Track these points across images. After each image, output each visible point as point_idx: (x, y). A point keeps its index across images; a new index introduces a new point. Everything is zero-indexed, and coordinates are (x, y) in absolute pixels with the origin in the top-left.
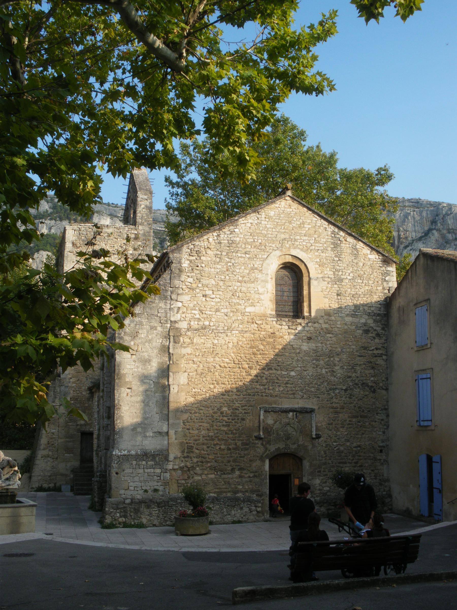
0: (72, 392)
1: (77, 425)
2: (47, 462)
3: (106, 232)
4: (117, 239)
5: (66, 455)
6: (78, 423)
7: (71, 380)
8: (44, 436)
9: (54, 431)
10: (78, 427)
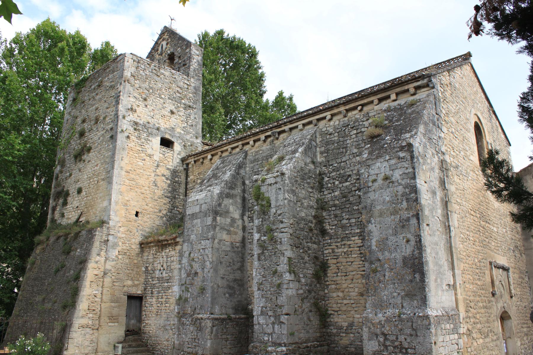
0: (120, 244)
1: (124, 286)
2: (85, 335)
3: (163, 74)
4: (172, 84)
5: (110, 324)
6: (125, 284)
7: (121, 229)
8: (84, 300)
9: (97, 292)
10: (125, 289)
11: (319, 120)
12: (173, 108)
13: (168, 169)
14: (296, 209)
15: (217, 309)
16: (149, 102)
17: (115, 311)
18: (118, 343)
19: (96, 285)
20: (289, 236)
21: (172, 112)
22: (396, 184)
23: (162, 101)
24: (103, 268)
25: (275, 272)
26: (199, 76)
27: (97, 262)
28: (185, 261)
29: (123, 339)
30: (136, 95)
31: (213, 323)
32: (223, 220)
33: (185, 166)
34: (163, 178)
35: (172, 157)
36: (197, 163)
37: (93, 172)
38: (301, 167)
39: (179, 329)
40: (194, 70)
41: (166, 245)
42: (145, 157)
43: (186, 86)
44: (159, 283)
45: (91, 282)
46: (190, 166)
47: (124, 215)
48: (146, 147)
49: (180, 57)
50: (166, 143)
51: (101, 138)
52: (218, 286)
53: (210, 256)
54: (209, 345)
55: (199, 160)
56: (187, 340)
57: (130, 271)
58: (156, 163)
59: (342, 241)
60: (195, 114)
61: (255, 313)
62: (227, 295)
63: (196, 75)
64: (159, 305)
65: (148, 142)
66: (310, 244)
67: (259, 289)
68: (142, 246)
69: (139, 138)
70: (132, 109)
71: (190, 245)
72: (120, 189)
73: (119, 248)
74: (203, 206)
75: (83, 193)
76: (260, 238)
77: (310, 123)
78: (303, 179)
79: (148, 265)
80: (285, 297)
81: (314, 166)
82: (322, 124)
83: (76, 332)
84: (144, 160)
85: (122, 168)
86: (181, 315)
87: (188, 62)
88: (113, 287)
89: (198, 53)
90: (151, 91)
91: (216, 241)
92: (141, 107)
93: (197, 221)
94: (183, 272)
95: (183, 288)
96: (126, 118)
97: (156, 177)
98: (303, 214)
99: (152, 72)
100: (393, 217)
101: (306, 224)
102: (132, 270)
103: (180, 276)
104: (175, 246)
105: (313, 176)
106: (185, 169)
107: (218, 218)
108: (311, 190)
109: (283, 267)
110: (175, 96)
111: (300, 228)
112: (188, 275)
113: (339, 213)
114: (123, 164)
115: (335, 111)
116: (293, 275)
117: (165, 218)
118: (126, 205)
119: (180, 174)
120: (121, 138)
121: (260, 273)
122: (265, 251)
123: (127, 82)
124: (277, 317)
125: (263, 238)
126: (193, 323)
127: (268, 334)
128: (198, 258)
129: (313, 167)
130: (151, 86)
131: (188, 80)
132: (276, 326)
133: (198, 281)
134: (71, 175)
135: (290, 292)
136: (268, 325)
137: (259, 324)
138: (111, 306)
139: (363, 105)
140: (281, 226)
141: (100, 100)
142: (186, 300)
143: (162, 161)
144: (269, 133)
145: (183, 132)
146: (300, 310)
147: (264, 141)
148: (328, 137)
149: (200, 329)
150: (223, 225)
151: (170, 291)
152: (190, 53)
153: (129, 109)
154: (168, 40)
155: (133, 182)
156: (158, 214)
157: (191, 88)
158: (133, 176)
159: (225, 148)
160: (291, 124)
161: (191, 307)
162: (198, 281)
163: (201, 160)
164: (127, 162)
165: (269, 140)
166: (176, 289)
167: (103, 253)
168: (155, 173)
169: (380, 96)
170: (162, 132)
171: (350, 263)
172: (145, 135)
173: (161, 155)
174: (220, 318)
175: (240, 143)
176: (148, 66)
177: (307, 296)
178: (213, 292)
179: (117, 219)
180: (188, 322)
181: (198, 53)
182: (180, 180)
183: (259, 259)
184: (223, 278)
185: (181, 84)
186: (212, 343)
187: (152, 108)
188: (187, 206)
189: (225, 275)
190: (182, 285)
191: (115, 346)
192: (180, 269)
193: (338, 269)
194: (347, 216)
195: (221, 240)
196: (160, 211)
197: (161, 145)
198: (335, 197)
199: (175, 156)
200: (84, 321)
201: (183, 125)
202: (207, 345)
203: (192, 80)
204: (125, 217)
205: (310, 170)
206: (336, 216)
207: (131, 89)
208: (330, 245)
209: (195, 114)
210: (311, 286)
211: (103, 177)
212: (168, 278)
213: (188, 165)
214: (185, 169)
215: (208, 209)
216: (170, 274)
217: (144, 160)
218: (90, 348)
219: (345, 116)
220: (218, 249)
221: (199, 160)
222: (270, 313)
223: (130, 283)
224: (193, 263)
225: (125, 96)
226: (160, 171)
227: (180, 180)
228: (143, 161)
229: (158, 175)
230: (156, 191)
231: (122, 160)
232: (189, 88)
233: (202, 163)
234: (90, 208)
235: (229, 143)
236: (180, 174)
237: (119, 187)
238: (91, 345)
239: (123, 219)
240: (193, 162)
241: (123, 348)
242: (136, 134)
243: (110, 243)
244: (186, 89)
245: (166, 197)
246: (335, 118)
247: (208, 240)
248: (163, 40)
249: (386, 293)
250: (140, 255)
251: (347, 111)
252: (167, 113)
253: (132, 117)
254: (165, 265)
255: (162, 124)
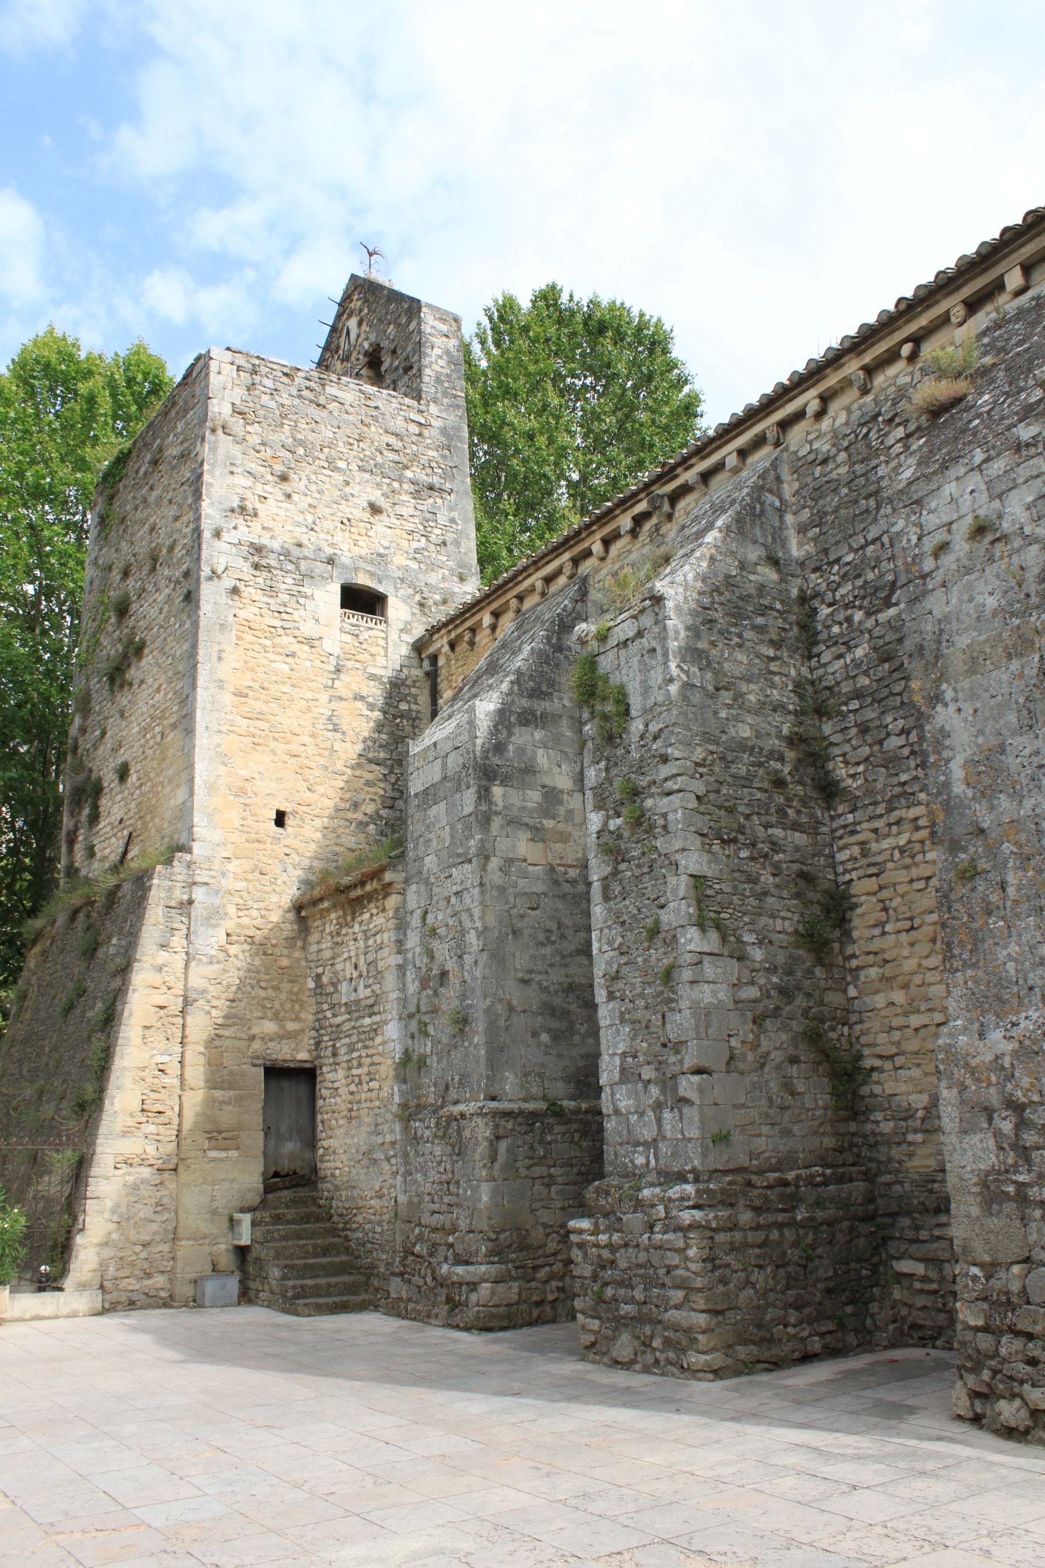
0: (232, 910)
1: (253, 1038)
3: (335, 399)
4: (368, 426)
6: (255, 1030)
7: (230, 867)
9: (166, 1059)
10: (257, 1045)
11: (784, 425)
12: (376, 496)
13: (372, 677)
14: (715, 713)
15: (510, 1083)
16: (297, 483)
17: (228, 1116)
18: (242, 1210)
19: (161, 1037)
20: (693, 804)
21: (375, 509)
22: (1017, 542)
23: (339, 478)
24: (181, 985)
25: (654, 931)
26: (455, 396)
27: (160, 969)
28: (413, 940)
29: (258, 1199)
30: (253, 466)
31: (496, 1127)
32: (515, 797)
33: (427, 665)
34: (359, 704)
35: (382, 642)
36: (458, 649)
37: (152, 711)
38: (728, 577)
39: (406, 1155)
40: (438, 380)
41: (359, 900)
42: (296, 648)
43: (414, 429)
44: (349, 1020)
45: (146, 1027)
46: (441, 661)
47: (237, 825)
48: (296, 615)
49: (394, 352)
50: (361, 600)
51: (166, 608)
52: (511, 1009)
53: (476, 913)
54: (485, 1198)
55: (460, 637)
56: (428, 1187)
57: (270, 992)
58: (333, 660)
59: (890, 810)
60: (451, 509)
61: (603, 1080)
62: (544, 1037)
63: (445, 394)
64: (353, 1088)
65: (302, 600)
66: (778, 832)
67: (611, 996)
68: (303, 914)
69: (271, 590)
70: (243, 509)
71: (423, 887)
72: (218, 746)
73: (230, 925)
74: (450, 760)
75: (133, 778)
76: (605, 824)
77: (759, 441)
78: (736, 614)
79: (320, 970)
80: (687, 1013)
81: (779, 571)
82: (796, 435)
83: (107, 1178)
84: (293, 655)
85: (221, 684)
86: (408, 1113)
87: (416, 357)
88: (217, 1043)
89: (444, 328)
90: (301, 451)
91: (494, 863)
92: (271, 501)
93: (438, 811)
94: (410, 975)
95: (414, 1026)
96: (225, 536)
97: (334, 705)
98: (745, 732)
99: (300, 397)
100: (1015, 665)
101: (760, 765)
102: (276, 988)
103: (403, 989)
104: (385, 897)
105: (778, 606)
106: (427, 674)
107: (497, 791)
108: (771, 653)
109: (677, 911)
110: (379, 459)
111: (735, 777)
112: (424, 983)
113: (873, 715)
114: (224, 670)
115: (832, 380)
116: (713, 935)
117: (372, 827)
118: (241, 792)
119: (413, 691)
120: (211, 596)
121: (610, 943)
122: (623, 866)
123: (220, 432)
124: (668, 1082)
125: (614, 824)
126: (440, 1133)
127: (646, 1144)
128: (447, 926)
129: (774, 576)
130: (299, 436)
131: (421, 412)
132: (667, 1115)
133: (449, 999)
134: (104, 733)
135: (706, 994)
136: (642, 1114)
137: (617, 1112)
138: (214, 1100)
139: (917, 340)
140: (665, 771)
141: (158, 503)
142: (422, 1063)
143: (351, 656)
144: (642, 506)
145: (414, 565)
146: (750, 1057)
147: (634, 533)
148: (818, 471)
149: (459, 1150)
150: (515, 812)
151: (379, 1040)
152: (420, 332)
153: (233, 511)
154: (361, 311)
155: (260, 724)
156: (350, 815)
157: (433, 435)
158: (258, 705)
159: (526, 584)
160: (703, 458)
161: (435, 1084)
162: (449, 999)
163: (467, 637)
164: (237, 665)
165: (648, 526)
166: (392, 1030)
167: (178, 941)
168: (331, 692)
169: (966, 291)
170: (344, 567)
171: (921, 884)
172: (290, 581)
173: (348, 638)
174: (521, 1112)
175: (567, 556)
176: (285, 380)
177: (777, 1008)
178: (492, 1028)
179: (217, 836)
180: (427, 1133)
181: (444, 328)
182: (414, 707)
183: (606, 898)
184: (525, 982)
185: (399, 424)
186: (495, 1193)
187: (309, 500)
188: (411, 770)
189: (531, 972)
190: (411, 1016)
191: (231, 1220)
192: (401, 968)
193: (885, 910)
194: (901, 723)
195: (510, 861)
196: (356, 806)
197: (343, 606)
198: (857, 664)
199: (393, 636)
200: (132, 1146)
201: (415, 545)
202: (480, 1200)
203: (433, 409)
204: (243, 829)
205: (761, 588)
206: (864, 729)
207: (236, 451)
208: (853, 832)
209: (451, 509)
210: (790, 972)
211: (172, 720)
212: (371, 1001)
213: (434, 659)
214: (427, 674)
215: (464, 766)
216: (376, 987)
217: (293, 655)
218: (155, 1227)
219: (865, 391)
220: (502, 890)
221: (460, 637)
222: (648, 1073)
223: (269, 1027)
224: (435, 944)
225: (218, 472)
226: (348, 686)
227: (414, 707)
228: (290, 660)
229: (341, 699)
230: (337, 746)
231: (220, 659)
232: (426, 432)
233: (472, 644)
234: (148, 818)
235: (535, 563)
236: (413, 691)
237: (217, 739)
238: (158, 1218)
239: (236, 837)
240: (446, 648)
241: (254, 1224)
242: (260, 580)
243: (197, 910)
244: (415, 439)
245: (370, 761)
246: (834, 407)
247: (470, 861)
248: (350, 316)
249: (1013, 948)
250: (299, 944)
251: (870, 371)
252: (357, 511)
253: (246, 532)
254: (362, 963)
255: (345, 547)
